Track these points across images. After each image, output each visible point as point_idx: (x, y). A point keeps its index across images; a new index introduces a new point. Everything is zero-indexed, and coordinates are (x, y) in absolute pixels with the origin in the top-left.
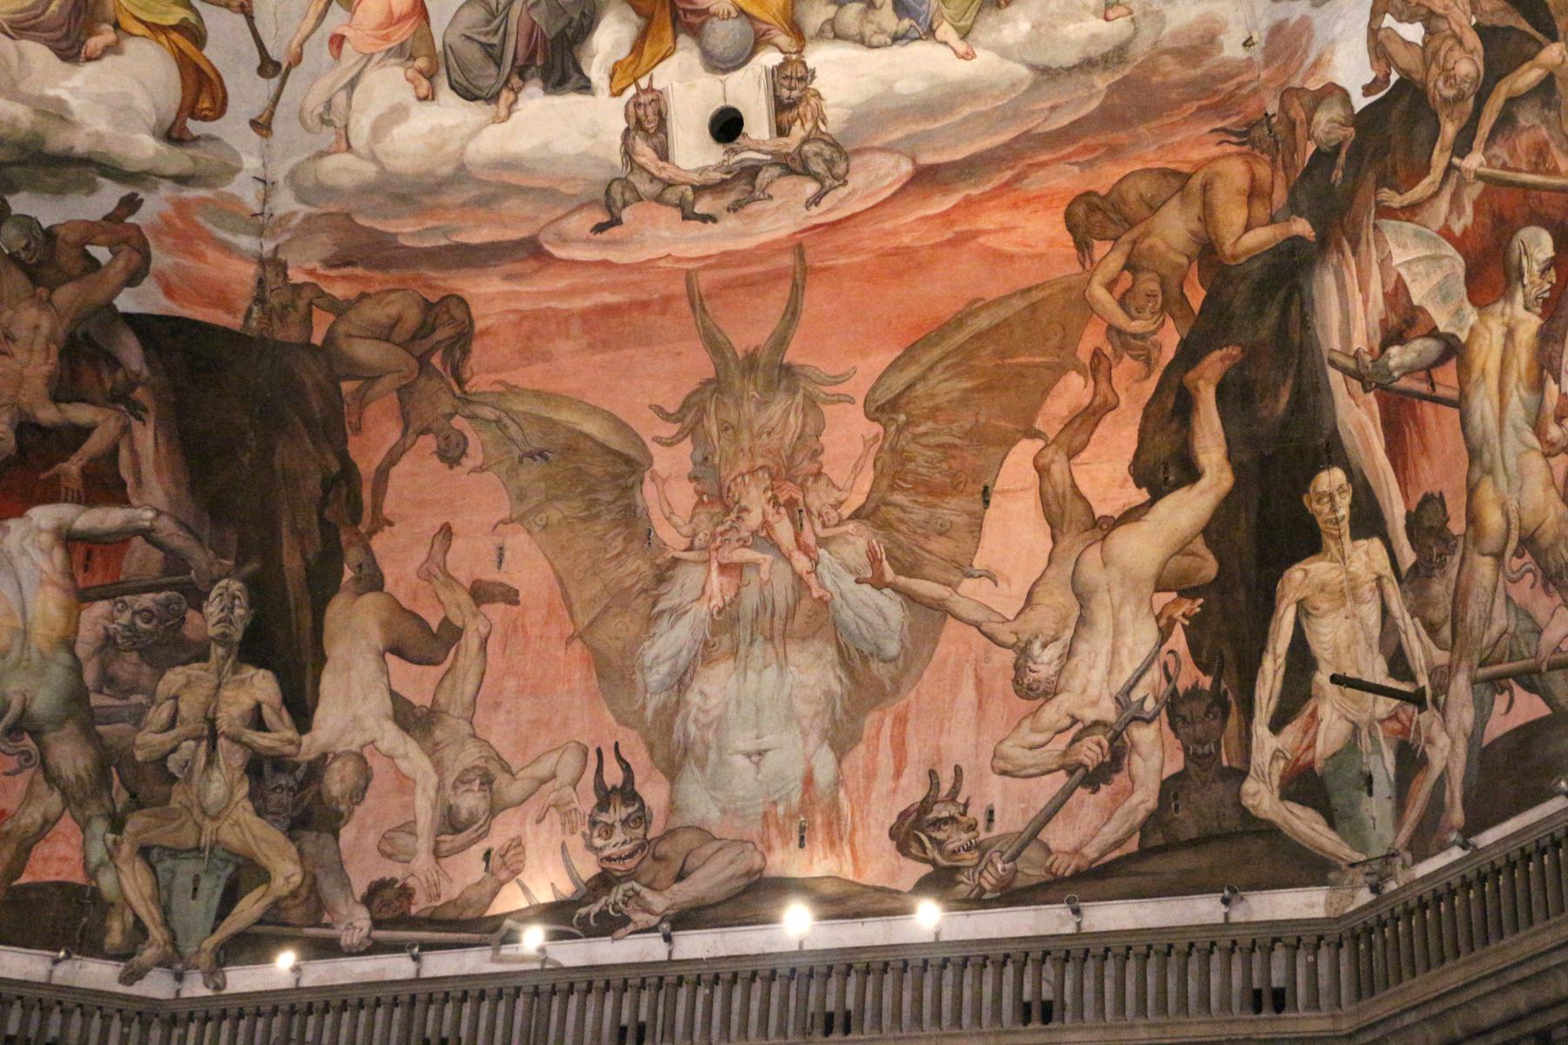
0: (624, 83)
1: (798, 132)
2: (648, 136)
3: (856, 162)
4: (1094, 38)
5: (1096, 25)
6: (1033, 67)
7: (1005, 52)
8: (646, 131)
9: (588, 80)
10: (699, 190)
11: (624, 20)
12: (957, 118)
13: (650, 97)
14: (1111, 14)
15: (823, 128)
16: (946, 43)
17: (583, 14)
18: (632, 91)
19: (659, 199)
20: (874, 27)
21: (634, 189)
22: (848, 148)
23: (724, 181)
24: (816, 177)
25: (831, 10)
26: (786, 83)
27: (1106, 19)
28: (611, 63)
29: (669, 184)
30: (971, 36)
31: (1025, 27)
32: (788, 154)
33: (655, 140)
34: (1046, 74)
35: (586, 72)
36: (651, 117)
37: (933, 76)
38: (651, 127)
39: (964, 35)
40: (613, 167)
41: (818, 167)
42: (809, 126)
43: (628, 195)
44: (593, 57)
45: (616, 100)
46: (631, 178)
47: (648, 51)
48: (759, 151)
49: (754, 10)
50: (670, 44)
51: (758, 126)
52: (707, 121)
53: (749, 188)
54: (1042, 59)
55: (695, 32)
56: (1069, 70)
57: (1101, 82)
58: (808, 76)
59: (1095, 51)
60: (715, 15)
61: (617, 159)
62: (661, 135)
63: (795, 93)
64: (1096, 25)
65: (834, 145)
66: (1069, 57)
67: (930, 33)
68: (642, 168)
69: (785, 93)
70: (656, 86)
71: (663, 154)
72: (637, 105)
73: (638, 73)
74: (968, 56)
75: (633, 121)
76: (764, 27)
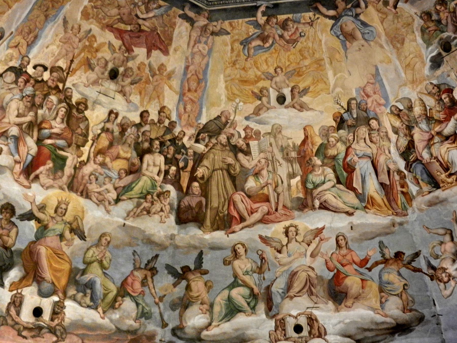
0: (14, 289)
1: (56, 322)
2: (15, 306)
3: (68, 336)
4: (131, 325)
5: (132, 322)
6: (116, 327)
7: (111, 321)
8: (15, 305)
9: (3, 283)
10: (25, 328)
11: (20, 271)
12: (96, 333)
13: (20, 296)
14: (137, 321)
15: (63, 323)
16: (99, 313)
17: (9, 264)
18: (15, 292)
19: (13, 327)
20: (84, 301)
21: (6, 321)
22: (68, 331)
23: (32, 328)
24: (57, 336)
25: (75, 292)
26: (57, 307)
27: (135, 322)
28: (12, 281)
29: (17, 323)
30: (106, 313)
31: (118, 316)
32: (51, 327)
33: (17, 309)
34: (119, 330)
35: (4, 281)
36: (18, 302)
37: (93, 320)
38: (17, 304)
39: (104, 312)
40: (2, 312)
41: (58, 333)
42: (59, 321)
43: (4, 322)
44: (7, 277)
45: (10, 293)
46: (7, 318)
47: (24, 282)
48: (44, 323)
49: (56, 283)
50: (31, 283)
51: (46, 316)
52: (33, 308)
53: (38, 332)
54: (119, 326)
55: (39, 283)
56: (124, 332)
57: (130, 337)
58: (64, 307)
59: (131, 329)
60: (46, 280)
61: (4, 310)
62: (19, 308)
63: (59, 311)
64: (132, 322)
65: (64, 329)
66: (125, 328)
67: (96, 309)
68: (11, 316)
69: (56, 310)
70: (23, 293)
71: (18, 314)
72: (15, 297)
73: (19, 287)
74: (103, 318)
75: (12, 301)
76: (57, 289)
